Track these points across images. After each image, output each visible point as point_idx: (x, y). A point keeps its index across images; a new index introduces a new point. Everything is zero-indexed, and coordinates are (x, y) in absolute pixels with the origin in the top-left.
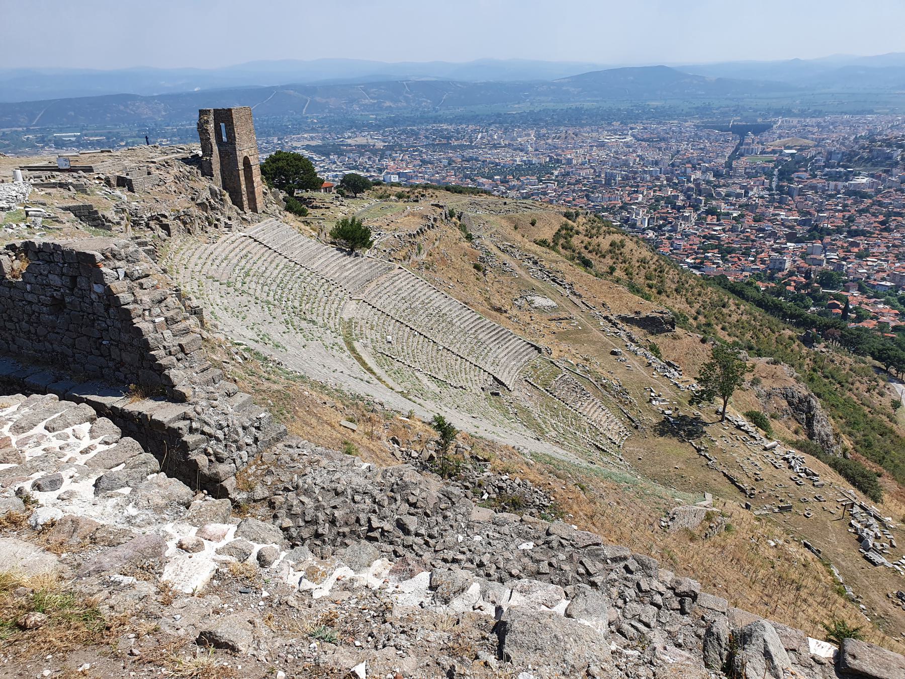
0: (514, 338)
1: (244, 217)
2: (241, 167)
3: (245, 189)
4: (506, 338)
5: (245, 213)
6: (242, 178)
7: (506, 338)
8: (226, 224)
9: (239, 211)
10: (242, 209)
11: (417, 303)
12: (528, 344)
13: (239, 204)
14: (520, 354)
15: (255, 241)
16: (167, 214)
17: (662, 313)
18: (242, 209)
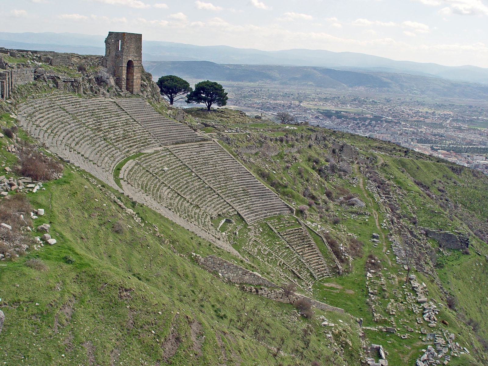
0: (276, 199)
1: (121, 93)
2: (125, 65)
3: (125, 78)
4: (270, 197)
5: (122, 91)
6: (125, 72)
7: (270, 197)
8: (103, 93)
9: (119, 90)
10: (121, 89)
11: (211, 161)
12: (286, 205)
13: (120, 86)
14: (274, 209)
15: (117, 105)
16: (61, 77)
17: (460, 234)
18: (121, 89)
